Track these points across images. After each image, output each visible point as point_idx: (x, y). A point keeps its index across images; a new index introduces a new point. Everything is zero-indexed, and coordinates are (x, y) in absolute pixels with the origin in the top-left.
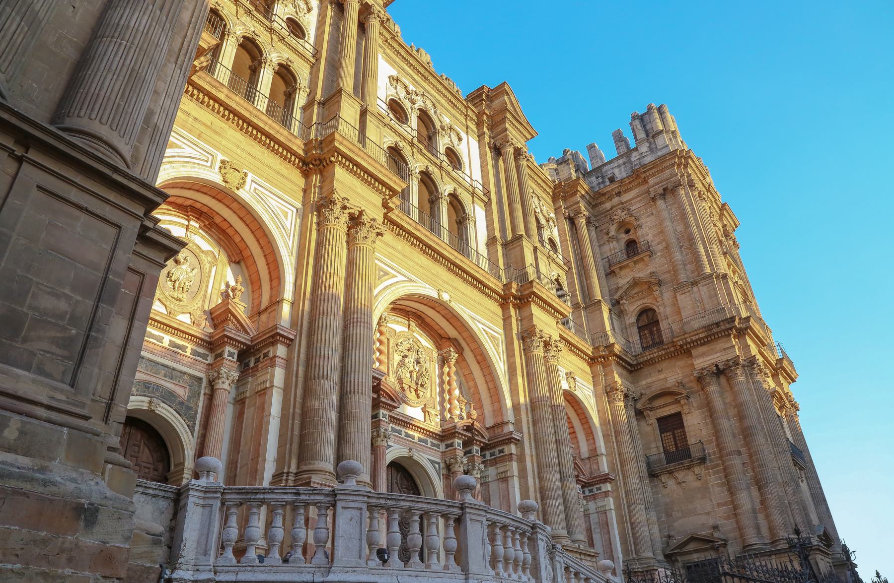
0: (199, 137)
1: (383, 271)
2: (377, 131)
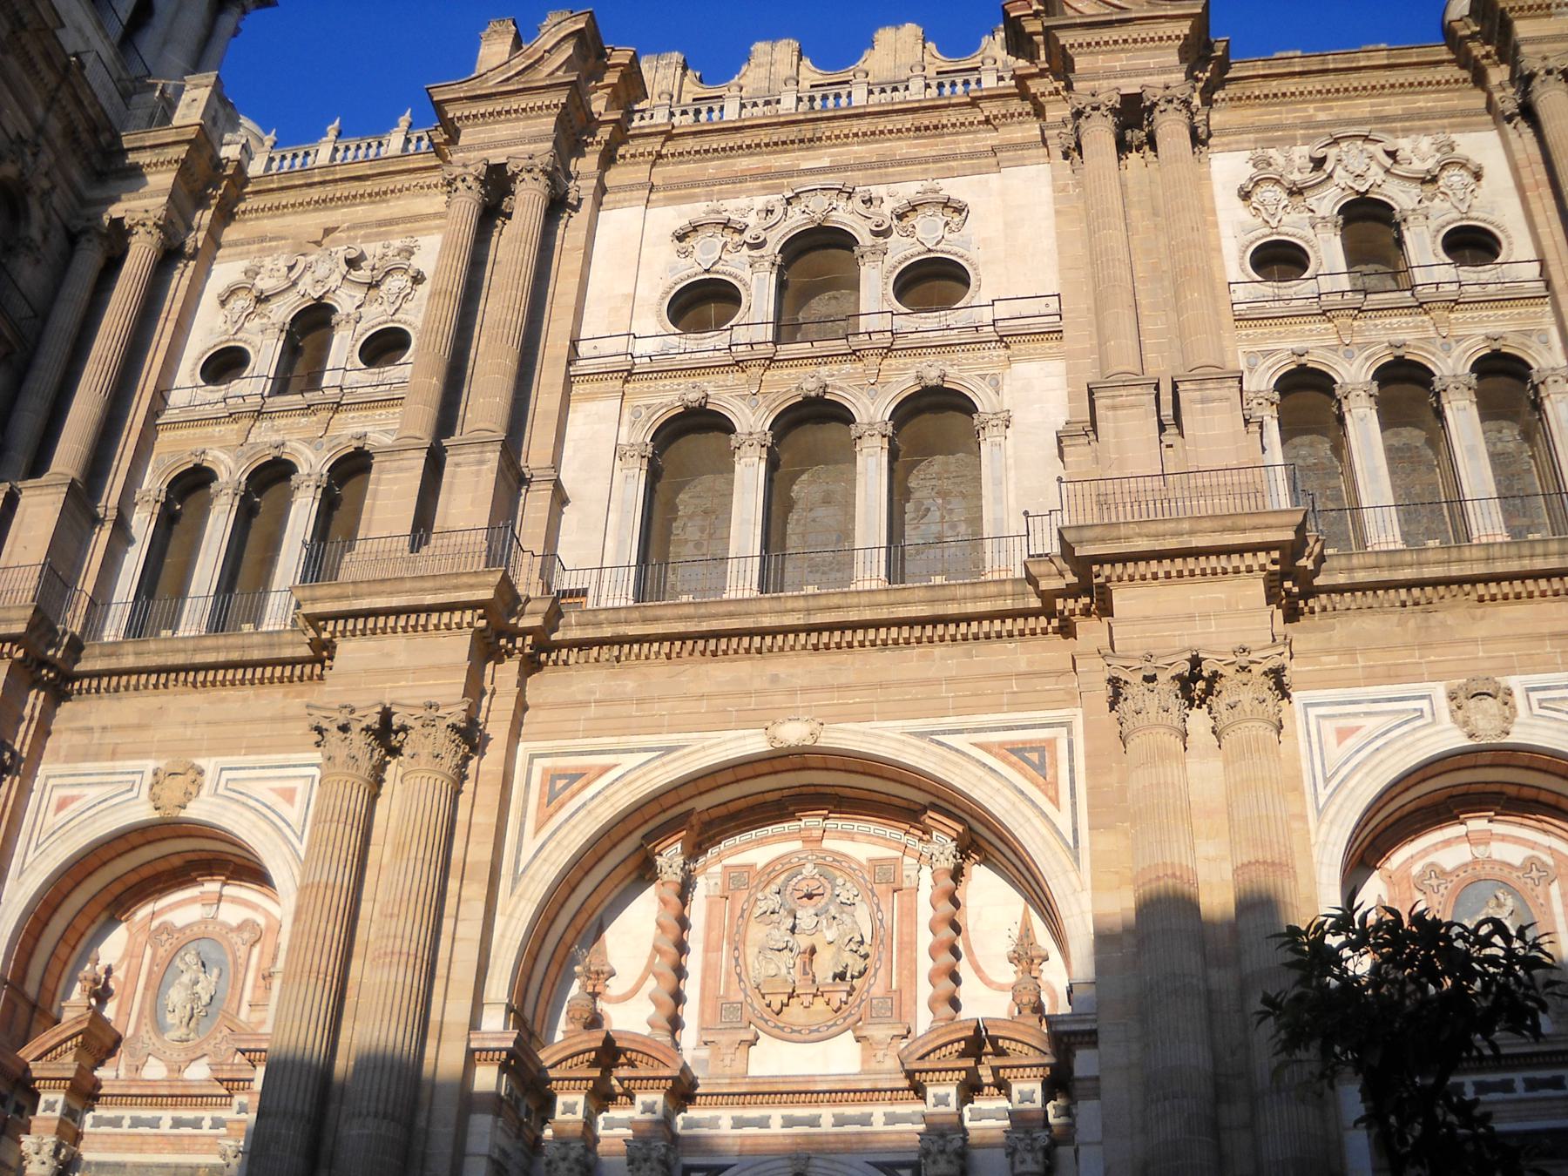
0: (114, 756)
1: (561, 777)
2: (478, 474)
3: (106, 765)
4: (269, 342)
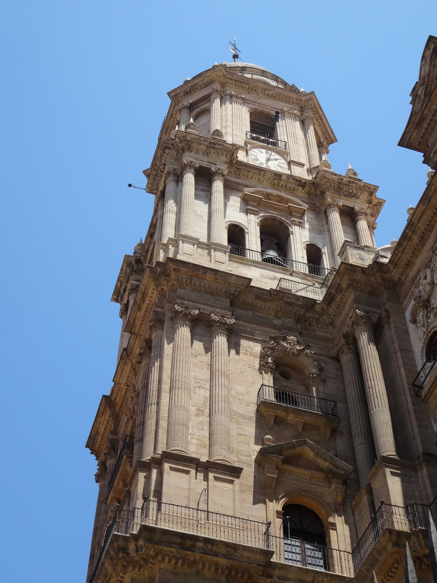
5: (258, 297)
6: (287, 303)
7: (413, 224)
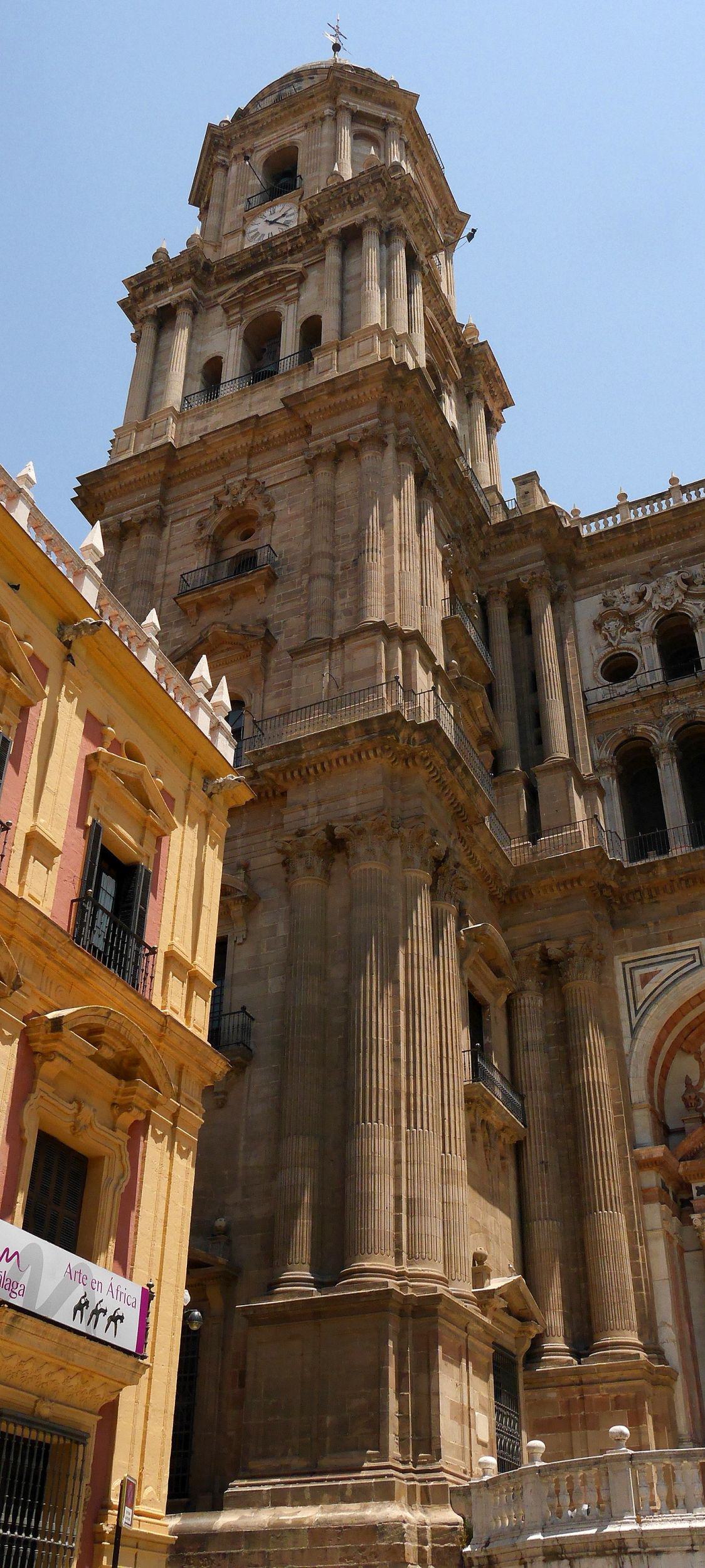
0: (671, 940)
3: (669, 948)
4: (647, 646)
5: (452, 478)
6: (469, 503)
7: (647, 524)
